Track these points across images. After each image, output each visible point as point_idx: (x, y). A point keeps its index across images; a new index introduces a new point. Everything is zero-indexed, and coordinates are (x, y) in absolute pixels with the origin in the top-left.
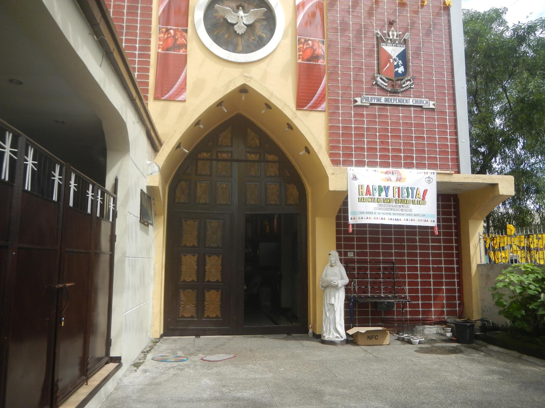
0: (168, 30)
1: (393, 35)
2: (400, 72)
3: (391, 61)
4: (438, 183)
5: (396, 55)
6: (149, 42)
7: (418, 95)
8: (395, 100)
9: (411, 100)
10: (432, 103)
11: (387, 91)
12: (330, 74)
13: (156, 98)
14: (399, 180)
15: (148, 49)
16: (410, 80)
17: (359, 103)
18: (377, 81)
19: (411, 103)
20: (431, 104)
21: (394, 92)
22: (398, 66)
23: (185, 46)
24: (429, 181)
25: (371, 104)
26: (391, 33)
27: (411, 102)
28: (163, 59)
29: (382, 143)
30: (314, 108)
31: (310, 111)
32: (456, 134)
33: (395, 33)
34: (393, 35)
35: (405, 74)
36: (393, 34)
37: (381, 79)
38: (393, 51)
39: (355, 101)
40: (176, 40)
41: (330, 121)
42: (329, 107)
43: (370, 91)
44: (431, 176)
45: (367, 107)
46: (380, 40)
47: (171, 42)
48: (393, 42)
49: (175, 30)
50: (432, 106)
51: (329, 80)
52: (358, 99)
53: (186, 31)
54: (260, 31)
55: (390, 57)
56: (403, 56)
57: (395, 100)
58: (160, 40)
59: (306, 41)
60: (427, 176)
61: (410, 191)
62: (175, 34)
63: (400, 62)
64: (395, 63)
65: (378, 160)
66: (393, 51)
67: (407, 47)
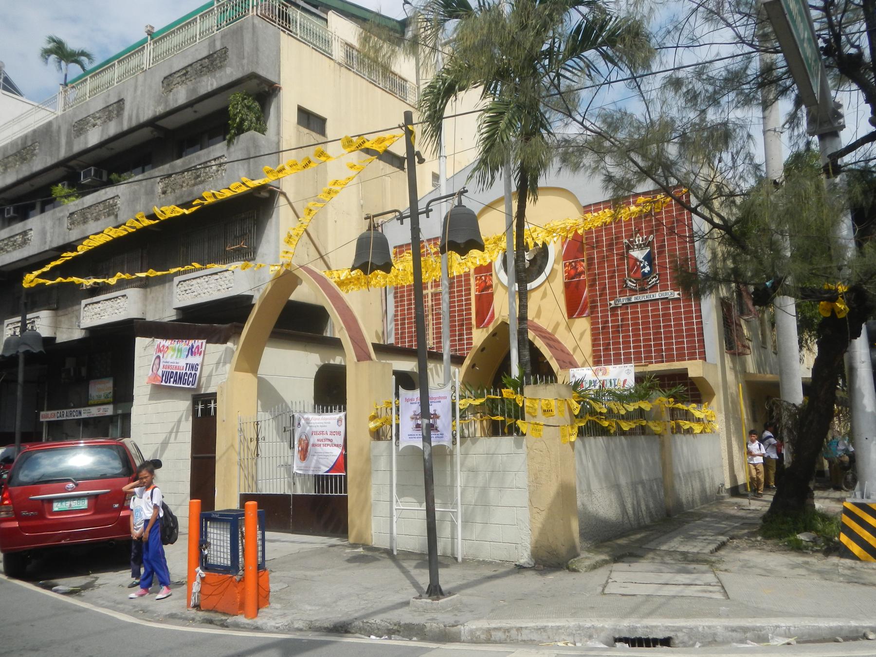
0: (481, 277)
1: (639, 240)
2: (646, 271)
3: (638, 263)
4: (635, 373)
5: (642, 257)
6: (470, 289)
7: (664, 288)
8: (643, 297)
9: (657, 294)
10: (676, 293)
11: (636, 291)
12: (590, 286)
13: (478, 327)
14: (604, 374)
15: (470, 294)
16: (655, 277)
17: (613, 305)
18: (627, 284)
19: (658, 297)
20: (676, 295)
21: (643, 290)
22: (644, 267)
23: (491, 286)
24: (628, 373)
25: (623, 304)
26: (637, 240)
27: (657, 295)
28: (478, 298)
29: (634, 336)
30: (580, 315)
31: (579, 317)
32: (701, 317)
33: (641, 239)
34: (639, 240)
35: (650, 272)
36: (638, 240)
37: (630, 281)
38: (638, 254)
39: (610, 304)
40: (486, 283)
41: (592, 324)
42: (592, 313)
43: (622, 292)
44: (630, 368)
45: (620, 307)
46: (628, 248)
47: (483, 285)
48: (640, 247)
49: (485, 276)
50: (676, 296)
51: (590, 291)
52: (612, 302)
53: (491, 275)
54: (539, 262)
55: (636, 260)
56: (649, 258)
57: (643, 297)
58: (476, 285)
59: (570, 263)
60: (627, 369)
61: (613, 381)
62: (486, 279)
63: (646, 263)
64: (642, 265)
65: (632, 350)
66: (638, 254)
67: (652, 248)
